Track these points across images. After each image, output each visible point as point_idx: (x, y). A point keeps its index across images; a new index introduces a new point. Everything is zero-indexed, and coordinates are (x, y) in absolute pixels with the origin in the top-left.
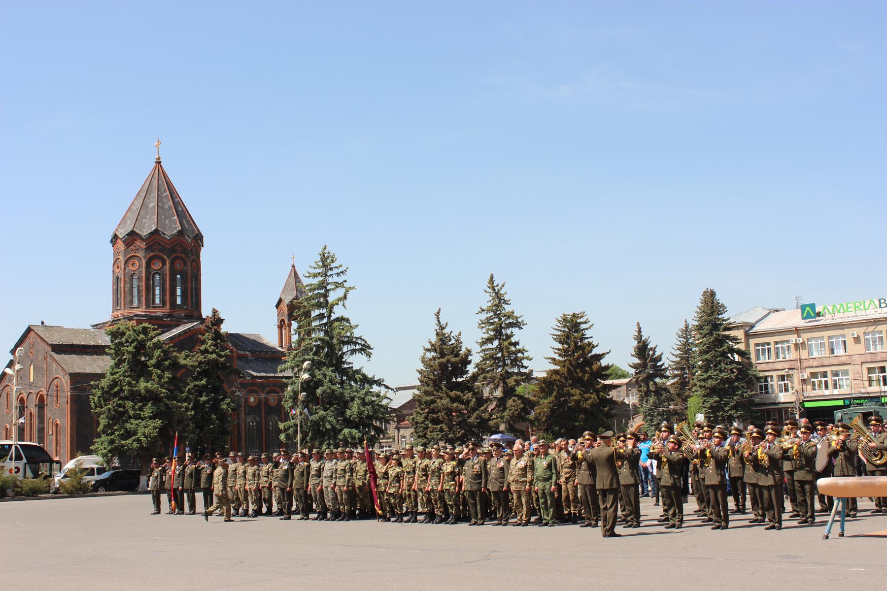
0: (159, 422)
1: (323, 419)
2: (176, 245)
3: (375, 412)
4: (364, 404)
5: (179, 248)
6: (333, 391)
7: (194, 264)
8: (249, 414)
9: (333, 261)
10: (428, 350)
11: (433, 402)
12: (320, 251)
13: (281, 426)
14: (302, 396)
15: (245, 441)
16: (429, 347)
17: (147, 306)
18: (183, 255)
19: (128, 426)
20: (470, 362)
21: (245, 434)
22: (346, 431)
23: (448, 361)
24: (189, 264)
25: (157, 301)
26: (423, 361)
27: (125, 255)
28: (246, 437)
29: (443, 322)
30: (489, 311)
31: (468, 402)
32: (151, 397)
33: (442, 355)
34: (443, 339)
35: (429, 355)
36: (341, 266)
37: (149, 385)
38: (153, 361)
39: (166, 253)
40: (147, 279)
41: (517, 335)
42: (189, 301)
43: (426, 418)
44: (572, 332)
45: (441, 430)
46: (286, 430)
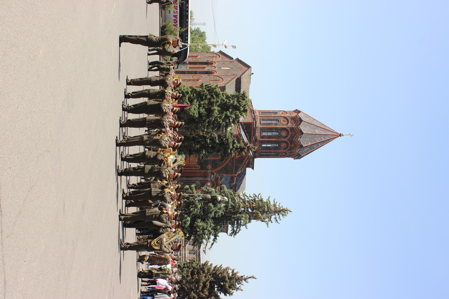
0: (197, 116)
1: (196, 207)
2: (295, 144)
3: (199, 235)
4: (203, 229)
5: (293, 145)
6: (211, 213)
7: (284, 154)
8: (201, 182)
9: (283, 215)
10: (233, 271)
11: (204, 272)
12: (289, 209)
13: (193, 186)
14: (209, 196)
15: (186, 180)
16: (235, 272)
17: (261, 129)
18: (289, 148)
19: (195, 101)
20: (225, 295)
21: (190, 180)
22: (189, 219)
23: (226, 282)
24: (284, 151)
25: (264, 134)
26: (228, 268)
27: (289, 117)
28: (188, 180)
29: (249, 280)
31: (203, 292)
32: (210, 112)
33: (230, 279)
34: (239, 280)
35: (230, 272)
36: (280, 220)
37: (216, 111)
38: (229, 114)
39: (288, 138)
42: (264, 151)
43: (194, 268)
45: (188, 276)
46: (191, 188)
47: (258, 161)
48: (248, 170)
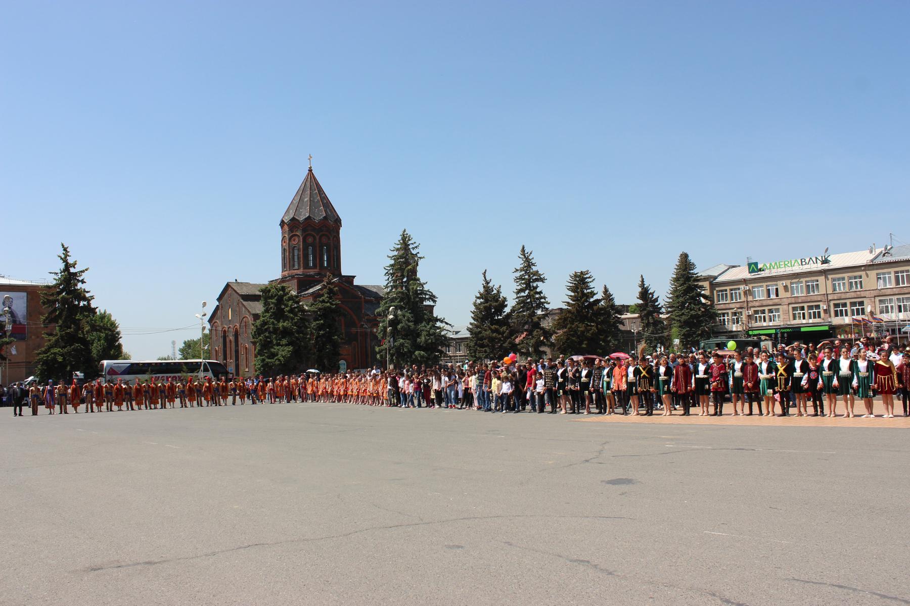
0: (291, 348)
1: (402, 345)
3: (436, 340)
4: (429, 335)
6: (409, 326)
10: (478, 298)
11: (480, 332)
12: (401, 233)
13: (377, 349)
14: (389, 329)
16: (478, 295)
19: (272, 350)
20: (506, 306)
22: (417, 353)
23: (490, 305)
26: (475, 304)
29: (488, 279)
30: (521, 271)
31: (504, 332)
32: (286, 333)
33: (487, 301)
34: (487, 289)
35: (479, 301)
37: (285, 324)
38: (288, 309)
39: (314, 233)
40: (304, 250)
41: (541, 287)
43: (476, 344)
44: (580, 282)
45: (485, 352)
46: (380, 352)
47: (345, 271)
48: (356, 282)
